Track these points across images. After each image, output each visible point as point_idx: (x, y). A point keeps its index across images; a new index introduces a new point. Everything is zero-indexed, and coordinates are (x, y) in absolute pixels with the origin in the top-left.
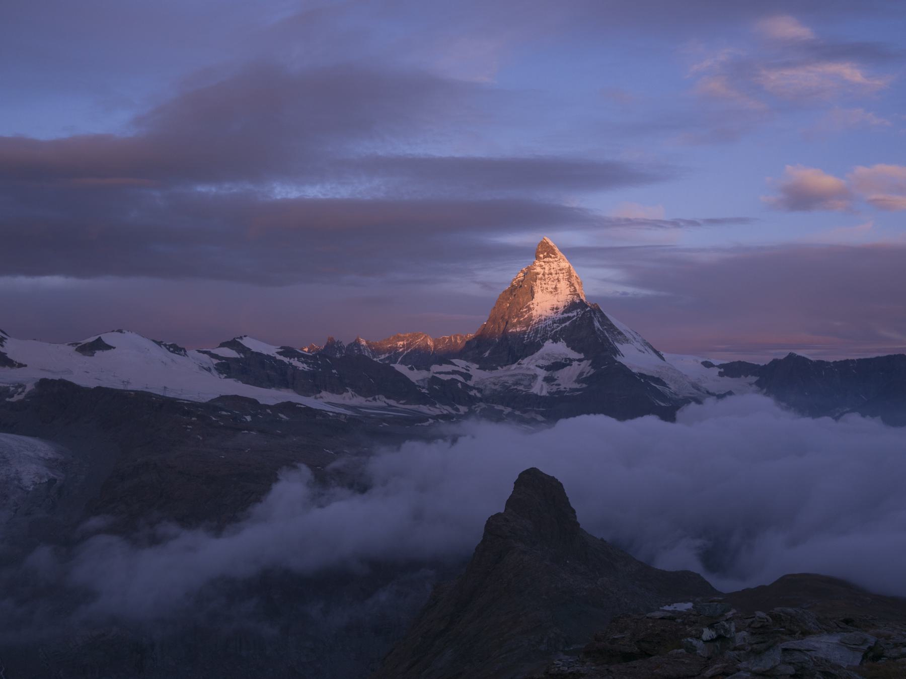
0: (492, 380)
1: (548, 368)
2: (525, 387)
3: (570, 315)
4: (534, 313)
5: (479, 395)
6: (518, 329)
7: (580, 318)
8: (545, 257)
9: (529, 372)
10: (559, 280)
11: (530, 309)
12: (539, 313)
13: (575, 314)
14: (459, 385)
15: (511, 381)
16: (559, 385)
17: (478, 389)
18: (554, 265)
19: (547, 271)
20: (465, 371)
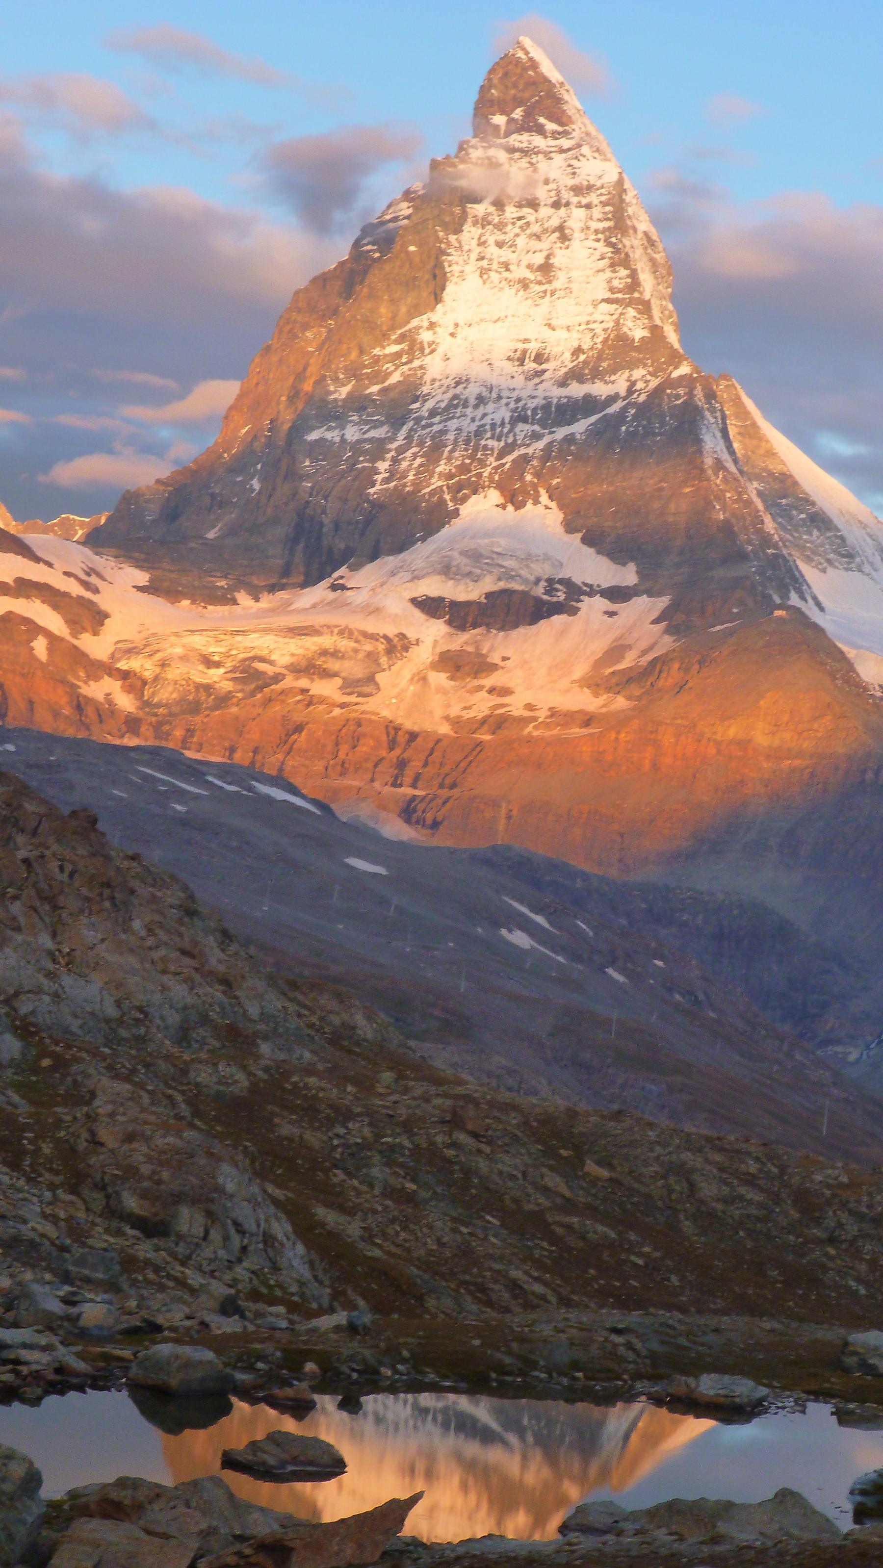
0: (198, 641)
1: (459, 615)
2: (350, 685)
4: (434, 367)
5: (125, 703)
6: (352, 433)
7: (644, 409)
9: (372, 626)
10: (563, 234)
11: (415, 348)
12: (456, 368)
14: (40, 646)
15: (282, 651)
16: (506, 692)
17: (125, 675)
18: (554, 168)
19: (514, 191)
20: (75, 589)
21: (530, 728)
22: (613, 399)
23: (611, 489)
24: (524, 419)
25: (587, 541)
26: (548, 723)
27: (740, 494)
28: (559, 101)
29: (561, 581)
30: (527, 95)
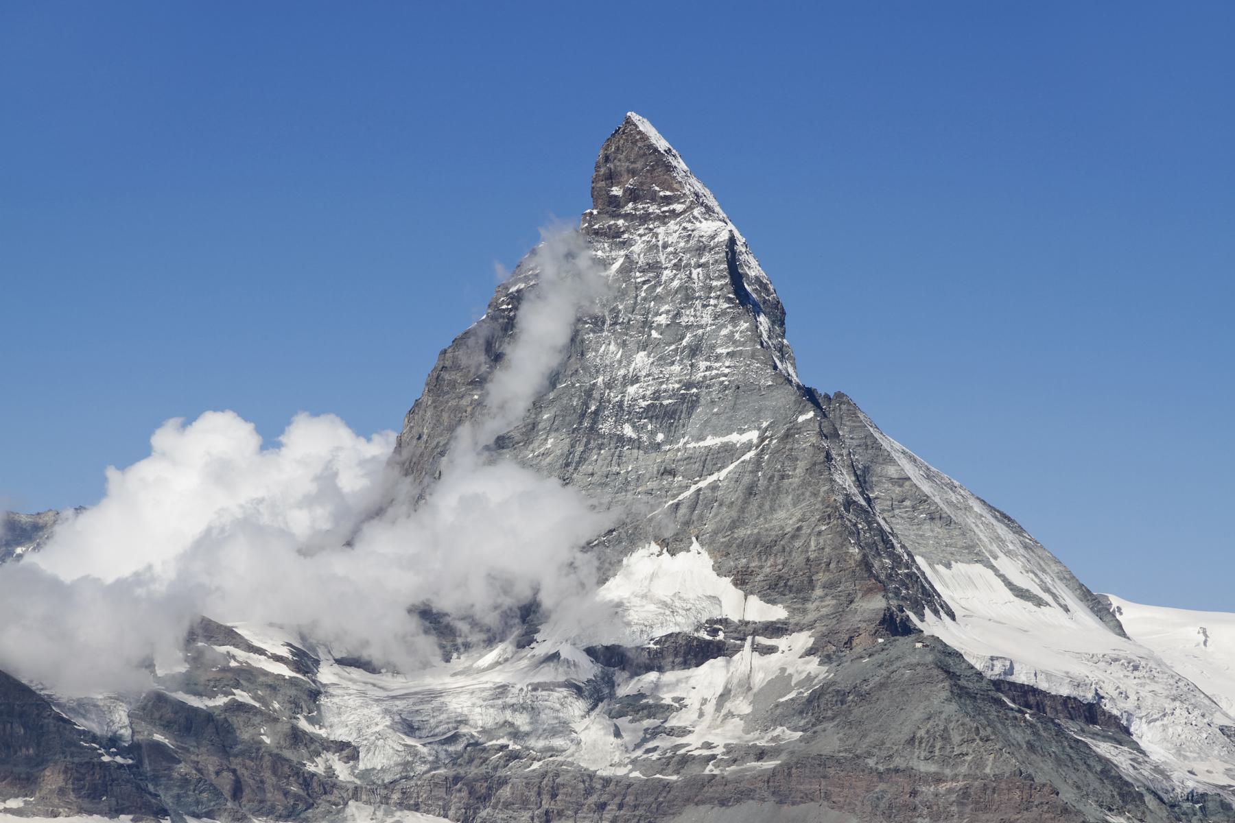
3: (735, 438)
8: (633, 195)
13: (753, 435)
16: (684, 732)
18: (670, 232)
21: (710, 766)
22: (748, 446)
23: (756, 531)
24: (672, 473)
25: (742, 580)
26: (725, 761)
27: (869, 523)
28: (669, 168)
29: (720, 621)
30: (639, 165)
